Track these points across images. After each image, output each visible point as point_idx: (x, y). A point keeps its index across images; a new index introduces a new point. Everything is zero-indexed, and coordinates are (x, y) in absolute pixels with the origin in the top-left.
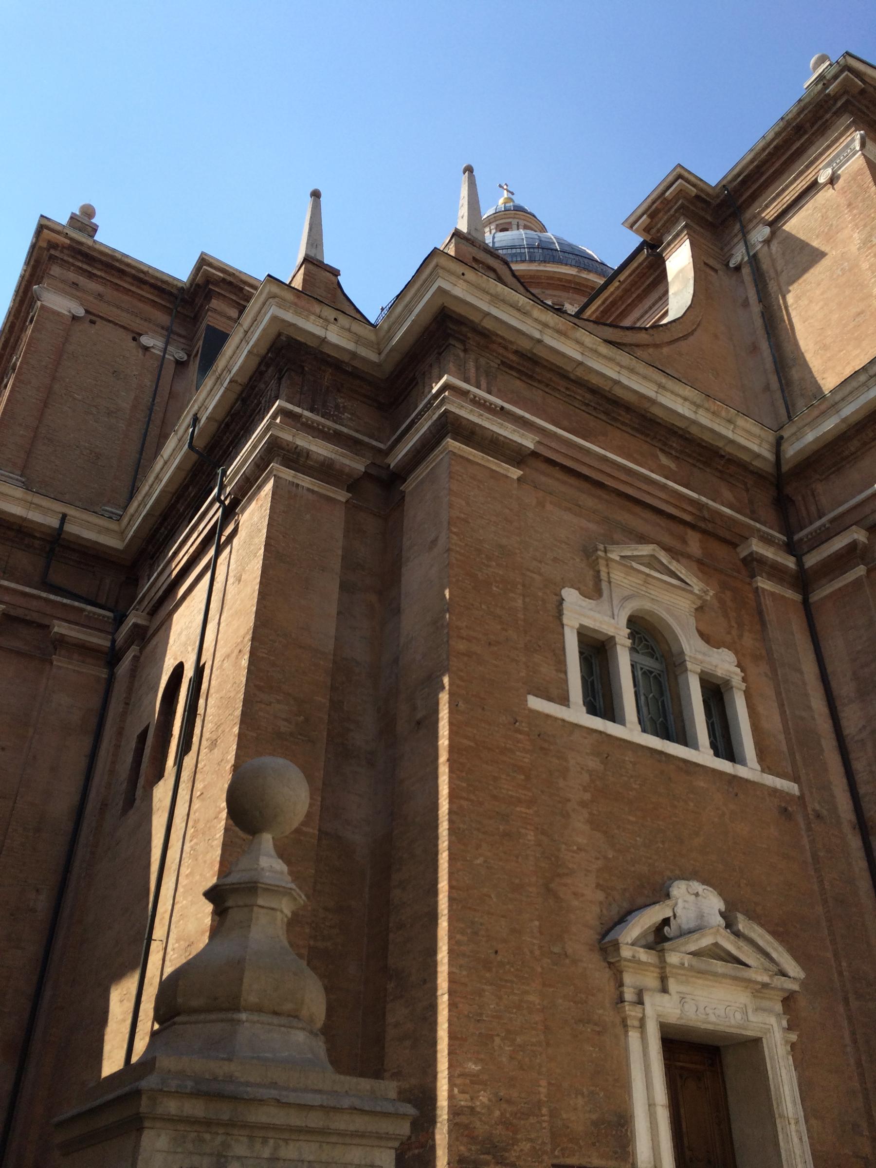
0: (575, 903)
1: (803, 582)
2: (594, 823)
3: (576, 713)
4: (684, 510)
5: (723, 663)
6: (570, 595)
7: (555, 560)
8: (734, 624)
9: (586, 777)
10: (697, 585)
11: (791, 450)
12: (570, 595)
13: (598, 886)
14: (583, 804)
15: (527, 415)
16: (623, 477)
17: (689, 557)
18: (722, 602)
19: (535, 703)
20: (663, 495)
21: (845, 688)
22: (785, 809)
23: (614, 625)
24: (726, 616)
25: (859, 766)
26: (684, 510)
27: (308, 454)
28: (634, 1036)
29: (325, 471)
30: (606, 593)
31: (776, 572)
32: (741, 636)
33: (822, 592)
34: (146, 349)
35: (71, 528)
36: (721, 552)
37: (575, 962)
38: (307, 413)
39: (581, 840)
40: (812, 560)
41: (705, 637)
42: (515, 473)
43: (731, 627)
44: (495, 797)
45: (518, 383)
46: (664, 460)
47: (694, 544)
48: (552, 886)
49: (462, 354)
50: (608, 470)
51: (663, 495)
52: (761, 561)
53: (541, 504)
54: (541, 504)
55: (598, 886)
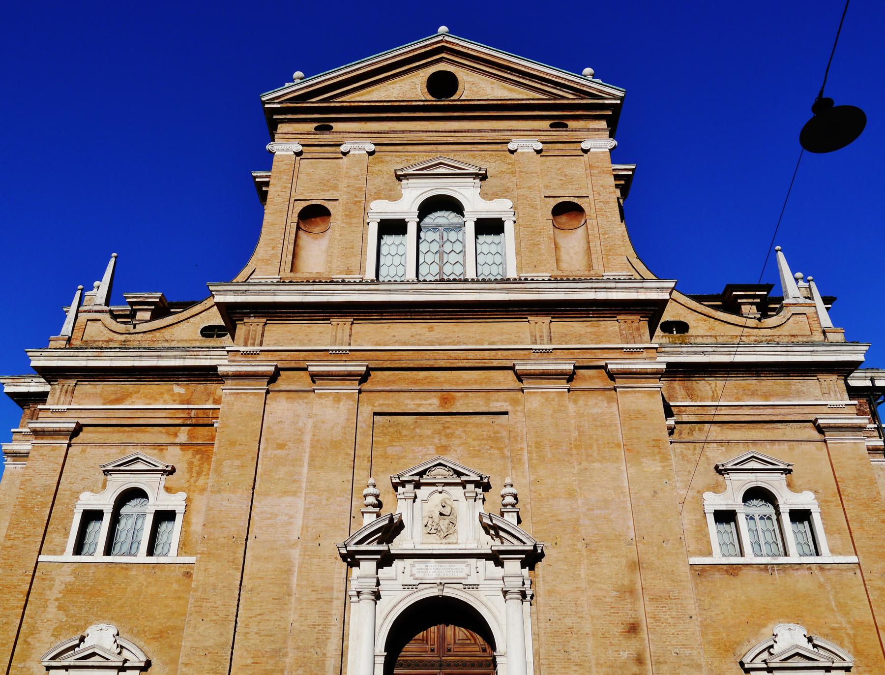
0: (38, 645)
2: (60, 608)
3: (68, 556)
4: (177, 418)
5: (175, 502)
7: (83, 479)
8: (194, 475)
9: (63, 586)
13: (52, 635)
14: (57, 600)
17: (175, 445)
18: (190, 464)
24: (190, 470)
26: (177, 418)
32: (195, 482)
37: (29, 669)
39: (50, 616)
41: (168, 489)
43: (191, 477)
44: (5, 609)
45: (89, 386)
47: (183, 435)
48: (29, 640)
50: (128, 414)
51: (164, 415)
53: (84, 451)
54: (84, 451)
55: (52, 635)
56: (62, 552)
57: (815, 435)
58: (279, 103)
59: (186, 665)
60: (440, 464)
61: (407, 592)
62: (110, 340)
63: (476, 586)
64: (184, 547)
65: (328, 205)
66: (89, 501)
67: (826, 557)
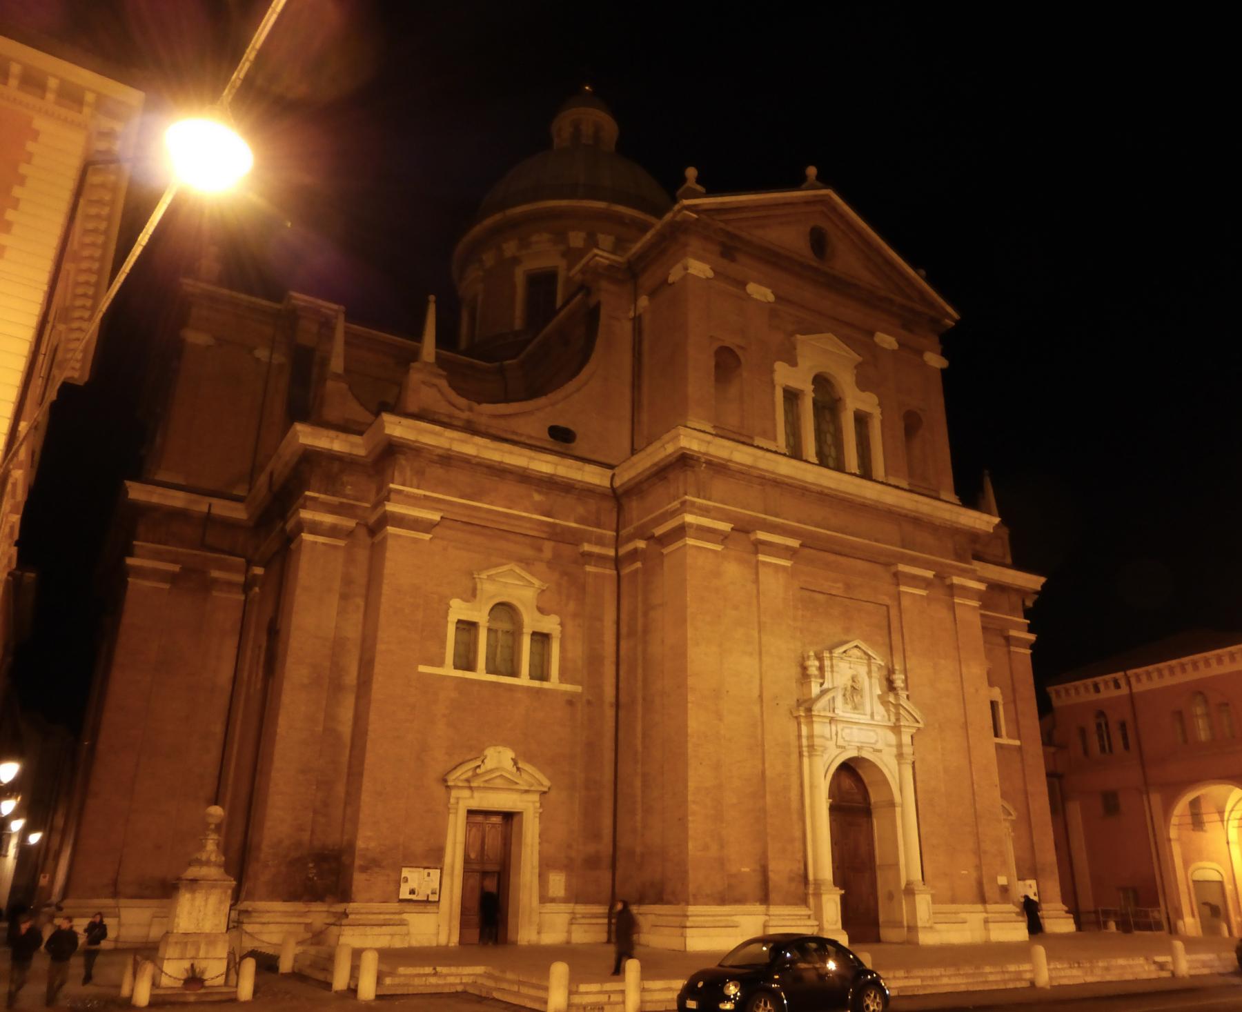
1: (618, 562)
3: (449, 670)
5: (550, 624)
6: (456, 603)
10: (537, 583)
11: (617, 483)
12: (456, 603)
15: (441, 496)
16: (503, 520)
19: (423, 669)
20: (528, 525)
21: (624, 630)
22: (571, 701)
23: (480, 615)
25: (622, 673)
27: (321, 523)
28: (452, 817)
29: (333, 531)
30: (478, 596)
31: (601, 559)
33: (626, 570)
34: (258, 360)
35: (215, 511)
36: (566, 550)
38: (322, 496)
40: (623, 551)
41: (541, 610)
42: (427, 537)
46: (537, 497)
49: (404, 462)
52: (589, 555)
53: (445, 549)
56: (441, 664)
57: (1002, 641)
58: (696, 212)
59: (694, 802)
60: (856, 647)
61: (839, 751)
62: (451, 416)
63: (880, 751)
64: (564, 675)
65: (739, 352)
66: (459, 610)
67: (1004, 741)
